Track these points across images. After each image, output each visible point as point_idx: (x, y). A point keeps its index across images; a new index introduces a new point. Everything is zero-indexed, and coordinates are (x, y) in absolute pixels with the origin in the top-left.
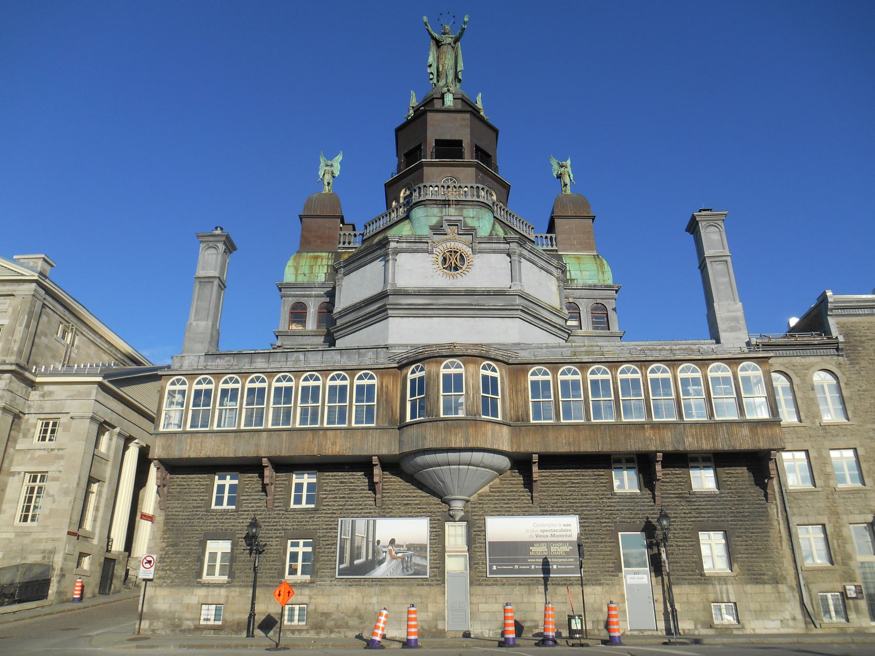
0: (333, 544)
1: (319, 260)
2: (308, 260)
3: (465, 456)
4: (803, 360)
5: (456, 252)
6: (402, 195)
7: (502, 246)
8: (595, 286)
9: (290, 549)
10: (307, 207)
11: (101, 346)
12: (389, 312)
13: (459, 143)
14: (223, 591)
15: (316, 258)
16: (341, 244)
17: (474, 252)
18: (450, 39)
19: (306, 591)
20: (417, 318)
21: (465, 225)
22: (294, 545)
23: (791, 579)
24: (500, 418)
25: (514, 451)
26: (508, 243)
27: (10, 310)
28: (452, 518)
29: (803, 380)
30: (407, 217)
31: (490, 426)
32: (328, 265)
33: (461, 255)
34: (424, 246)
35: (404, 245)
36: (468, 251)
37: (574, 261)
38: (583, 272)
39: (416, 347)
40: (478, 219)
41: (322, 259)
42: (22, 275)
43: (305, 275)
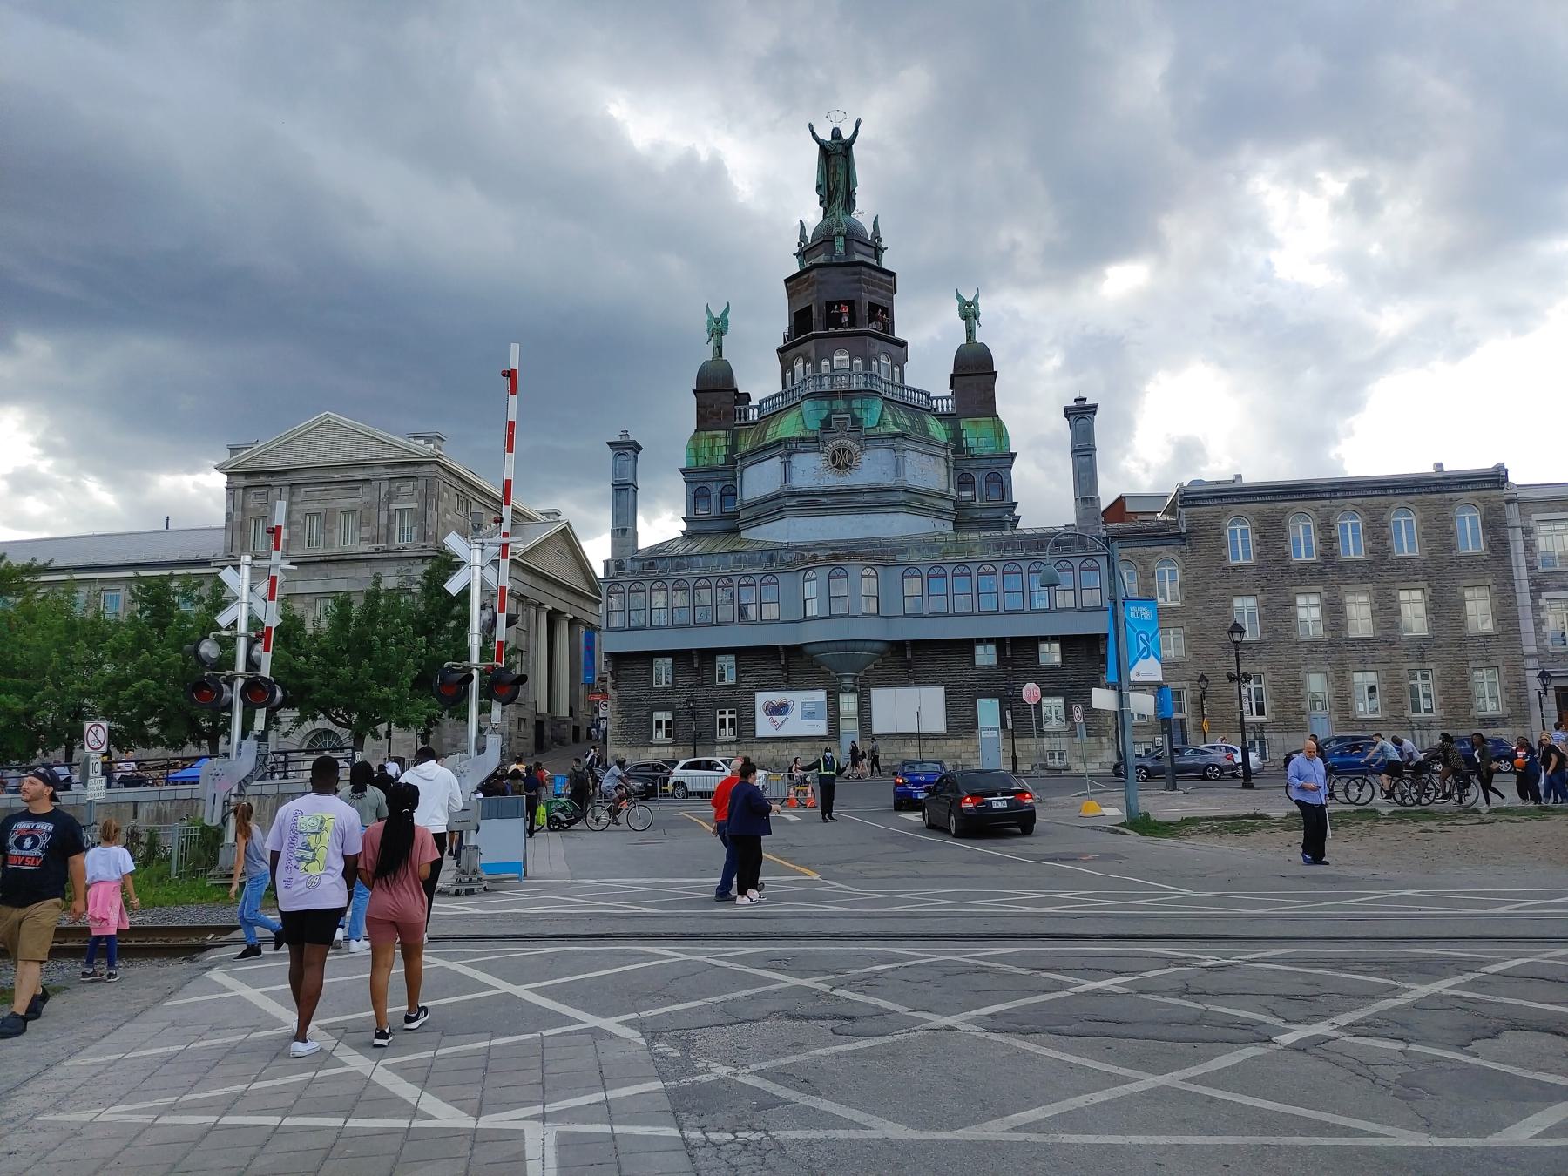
0: (751, 712)
1: (718, 440)
4: (1148, 549)
5: (845, 450)
9: (719, 717)
10: (699, 380)
12: (787, 512)
14: (671, 749)
15: (714, 437)
16: (737, 420)
17: (861, 450)
19: (734, 747)
22: (724, 713)
23: (1112, 733)
27: (416, 492)
28: (845, 690)
29: (1146, 568)
37: (971, 426)
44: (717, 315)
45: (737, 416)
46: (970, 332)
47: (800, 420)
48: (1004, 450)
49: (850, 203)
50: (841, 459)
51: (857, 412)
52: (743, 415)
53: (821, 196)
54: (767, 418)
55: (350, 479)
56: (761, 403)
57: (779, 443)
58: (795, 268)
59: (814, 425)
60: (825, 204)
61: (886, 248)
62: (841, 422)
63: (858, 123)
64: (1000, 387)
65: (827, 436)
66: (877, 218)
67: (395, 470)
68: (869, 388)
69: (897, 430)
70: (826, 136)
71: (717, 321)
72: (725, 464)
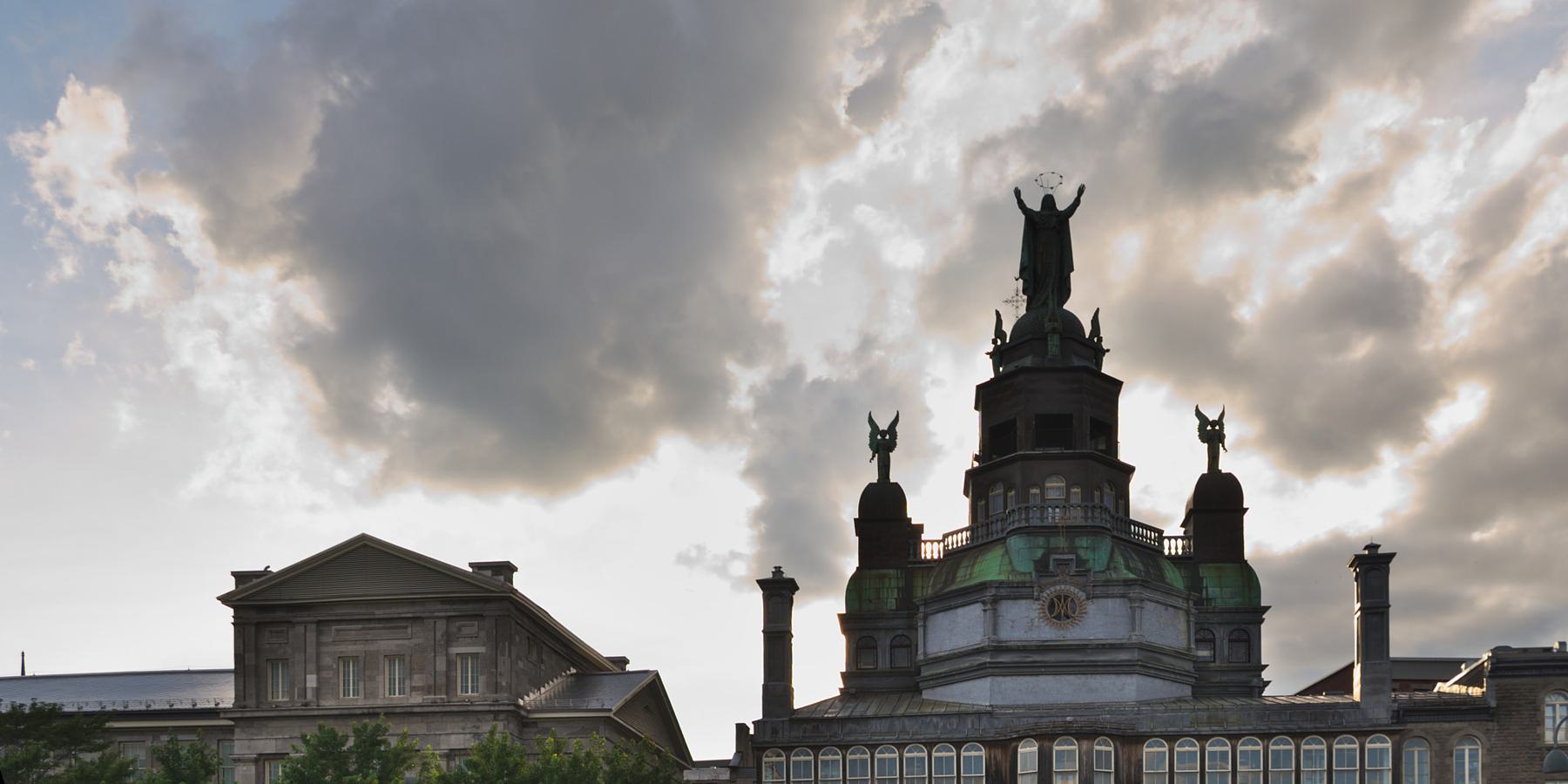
1: (887, 580)
4: (1446, 725)
5: (1066, 598)
15: (882, 577)
16: (912, 556)
17: (1088, 599)
30: (1004, 539)
32: (898, 588)
36: (1082, 595)
38: (1224, 589)
40: (1094, 550)
41: (890, 579)
42: (487, 590)
43: (870, 601)
44: (883, 425)
45: (911, 551)
47: (1006, 560)
51: (1082, 553)
54: (953, 557)
55: (395, 616)
57: (983, 586)
58: (986, 372)
59: (1025, 566)
62: (1062, 563)
65: (1044, 581)
67: (455, 607)
69: (1132, 576)
71: (883, 433)
72: (896, 610)
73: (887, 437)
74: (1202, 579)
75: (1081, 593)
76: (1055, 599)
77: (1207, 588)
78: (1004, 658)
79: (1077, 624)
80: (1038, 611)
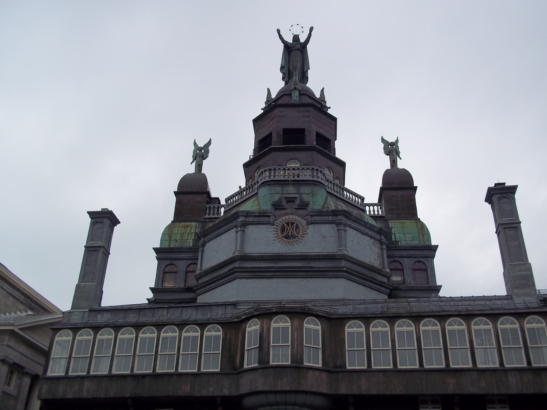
1: (189, 228)
2: (180, 229)
3: (291, 398)
5: (292, 224)
6: (256, 175)
7: (331, 218)
8: (416, 247)
11: (19, 298)
12: (237, 274)
13: (301, 132)
15: (186, 227)
16: (207, 215)
18: (299, 45)
20: (260, 279)
21: (301, 200)
24: (320, 365)
25: (332, 393)
26: (336, 215)
31: (311, 373)
32: (196, 233)
33: (297, 224)
34: (266, 219)
35: (251, 219)
36: (304, 222)
38: (406, 235)
39: (258, 303)
40: (313, 195)
44: (201, 144)
45: (207, 212)
46: (393, 163)
47: (256, 203)
48: (427, 243)
49: (304, 78)
50: (290, 231)
51: (306, 198)
52: (212, 212)
53: (284, 73)
56: (227, 200)
59: (267, 206)
60: (286, 79)
61: (330, 108)
63: (311, 29)
64: (420, 198)
65: (278, 213)
66: (323, 89)
68: (315, 179)
70: (289, 39)
71: (200, 149)
73: (203, 151)
74: (391, 228)
75: (303, 220)
76: (285, 225)
77: (395, 234)
78: (248, 265)
79: (300, 242)
80: (273, 233)
